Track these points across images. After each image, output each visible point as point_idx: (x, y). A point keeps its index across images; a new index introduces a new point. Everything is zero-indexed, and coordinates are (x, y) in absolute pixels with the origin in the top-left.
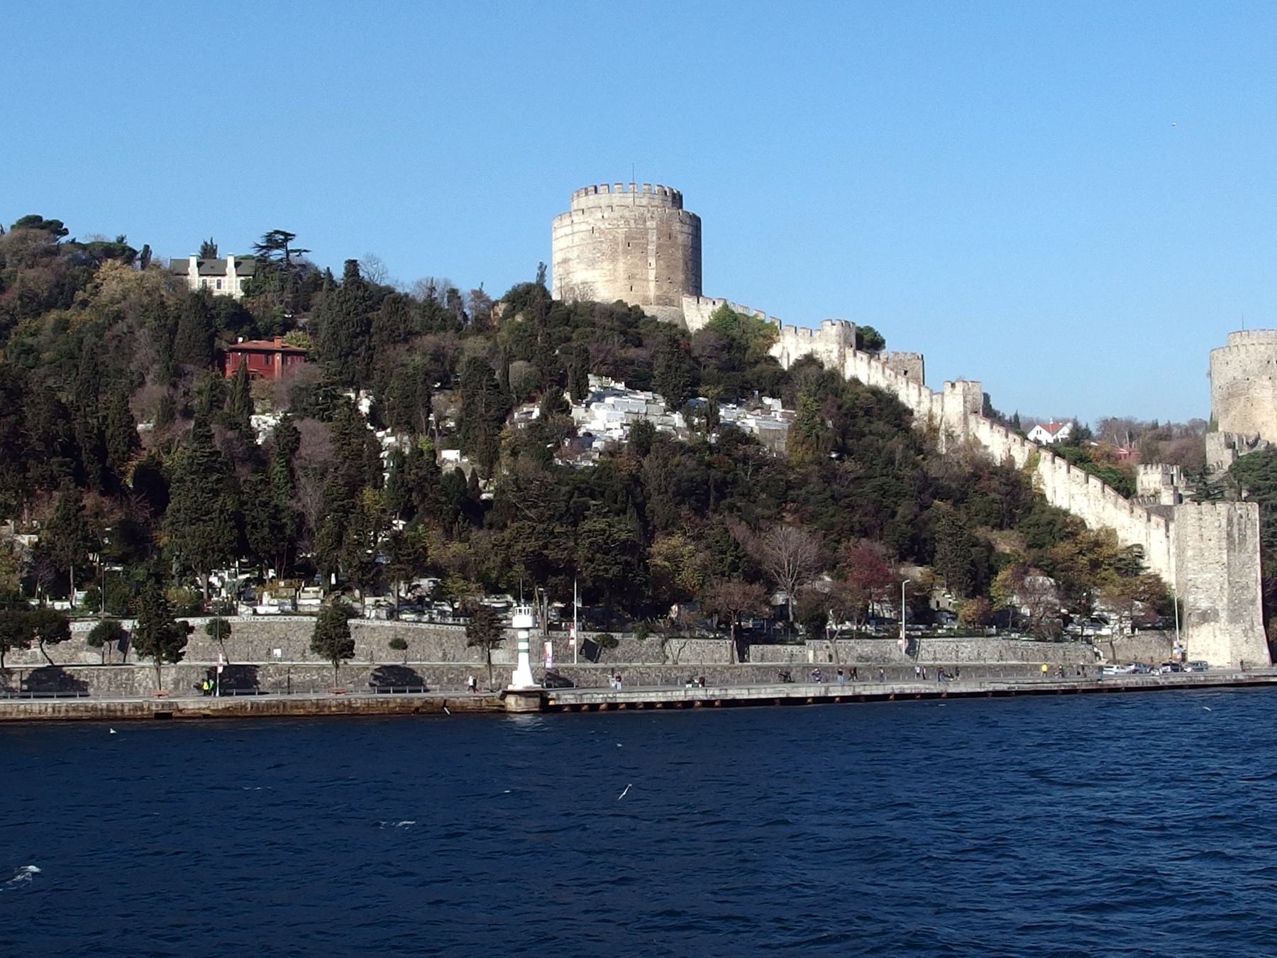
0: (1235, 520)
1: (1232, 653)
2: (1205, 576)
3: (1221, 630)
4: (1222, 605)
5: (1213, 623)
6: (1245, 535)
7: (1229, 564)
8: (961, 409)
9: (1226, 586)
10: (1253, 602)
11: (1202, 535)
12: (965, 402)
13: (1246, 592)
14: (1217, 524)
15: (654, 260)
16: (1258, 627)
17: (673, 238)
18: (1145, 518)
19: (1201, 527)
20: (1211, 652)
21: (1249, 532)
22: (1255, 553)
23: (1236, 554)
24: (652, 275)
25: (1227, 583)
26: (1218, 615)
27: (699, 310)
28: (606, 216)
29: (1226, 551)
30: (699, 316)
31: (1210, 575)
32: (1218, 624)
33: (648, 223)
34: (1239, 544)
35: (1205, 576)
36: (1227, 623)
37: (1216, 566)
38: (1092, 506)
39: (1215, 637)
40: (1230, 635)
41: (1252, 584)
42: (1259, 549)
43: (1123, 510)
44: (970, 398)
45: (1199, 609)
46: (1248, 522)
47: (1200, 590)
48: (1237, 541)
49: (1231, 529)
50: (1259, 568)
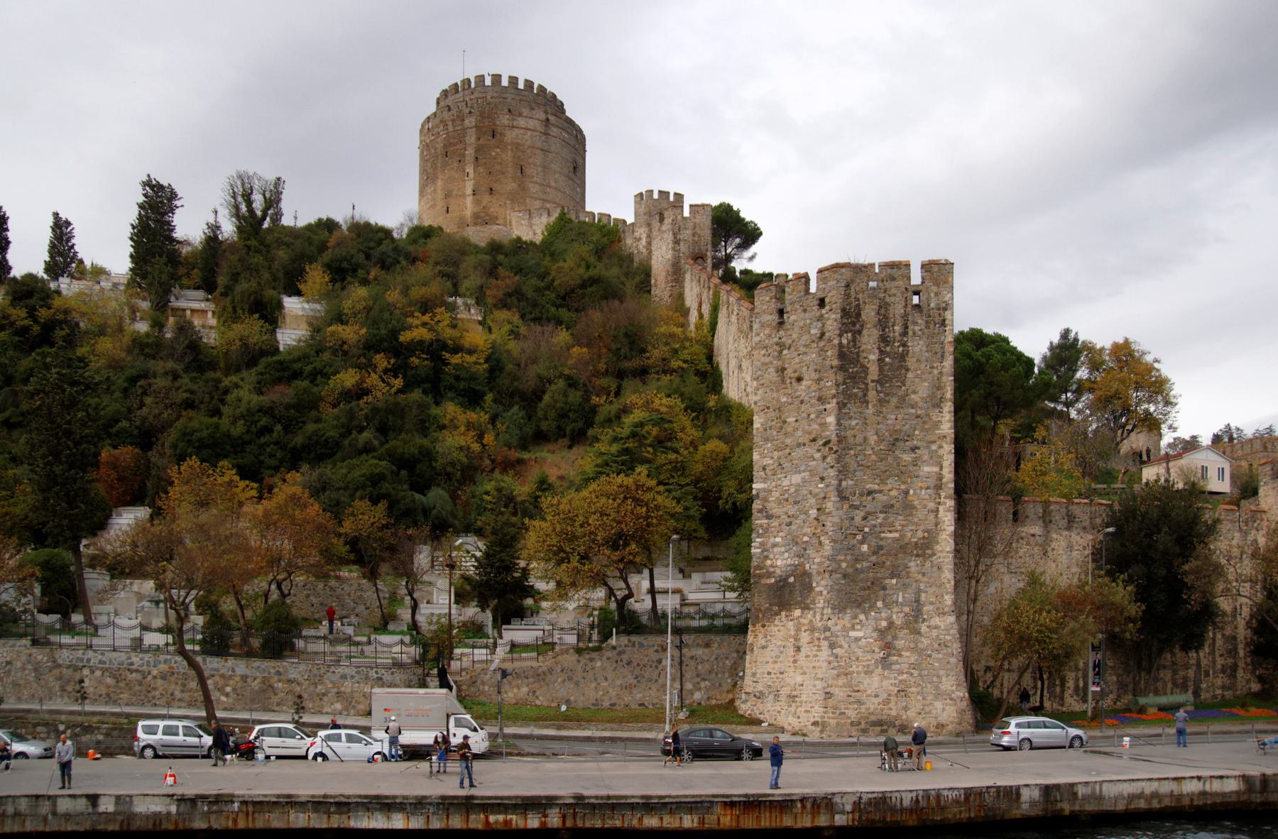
1: (828, 695)
2: (786, 483)
3: (812, 629)
5: (797, 613)
6: (903, 357)
7: (841, 439)
9: (829, 506)
11: (783, 369)
13: (899, 521)
17: (498, 136)
19: (781, 346)
20: (785, 691)
21: (917, 346)
22: (938, 405)
25: (833, 497)
26: (811, 589)
29: (832, 405)
31: (796, 479)
36: (828, 611)
37: (810, 450)
39: (798, 649)
40: (832, 646)
42: (949, 393)
45: (769, 575)
47: (775, 523)
50: (947, 453)
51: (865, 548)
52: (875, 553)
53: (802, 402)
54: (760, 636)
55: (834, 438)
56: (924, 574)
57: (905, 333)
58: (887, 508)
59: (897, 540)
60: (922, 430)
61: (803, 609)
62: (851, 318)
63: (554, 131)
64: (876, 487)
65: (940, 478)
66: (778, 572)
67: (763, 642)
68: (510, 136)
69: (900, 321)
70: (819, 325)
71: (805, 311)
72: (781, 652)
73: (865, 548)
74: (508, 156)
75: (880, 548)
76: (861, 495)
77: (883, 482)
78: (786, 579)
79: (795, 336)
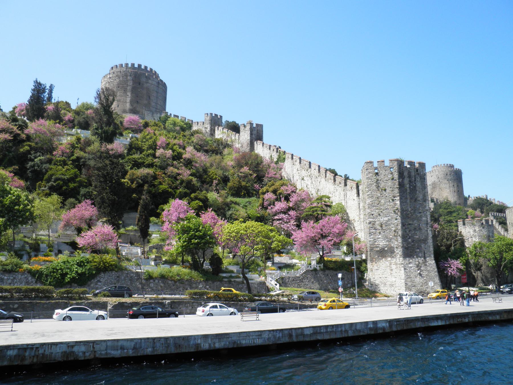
0: (406, 174)
1: (406, 284)
3: (396, 264)
4: (397, 243)
5: (389, 259)
8: (249, 138)
10: (425, 241)
12: (251, 134)
14: (390, 176)
15: (130, 93)
16: (430, 262)
18: (343, 184)
21: (419, 184)
23: (408, 201)
24: (128, 100)
27: (153, 116)
28: (111, 76)
29: (398, 198)
30: (153, 119)
31: (386, 219)
32: (394, 260)
33: (129, 78)
34: (410, 193)
35: (382, 220)
38: (314, 182)
40: (405, 269)
41: (423, 226)
43: (330, 181)
44: (255, 132)
45: (377, 247)
46: (417, 176)
48: (408, 191)
49: (403, 181)
51: (410, 240)
52: (413, 242)
53: (386, 196)
54: (375, 266)
55: (399, 208)
56: (426, 248)
57: (415, 180)
58: (415, 229)
59: (417, 238)
60: (422, 207)
61: (391, 258)
62: (401, 174)
63: (161, 86)
64: (411, 223)
65: (427, 221)
66: (380, 246)
67: (377, 268)
68: (146, 85)
69: (413, 177)
70: (391, 175)
71: (386, 171)
72: (385, 271)
73: (410, 240)
74: (145, 92)
75: (414, 240)
76: (408, 225)
77: (413, 221)
78: (384, 249)
79: (382, 177)
